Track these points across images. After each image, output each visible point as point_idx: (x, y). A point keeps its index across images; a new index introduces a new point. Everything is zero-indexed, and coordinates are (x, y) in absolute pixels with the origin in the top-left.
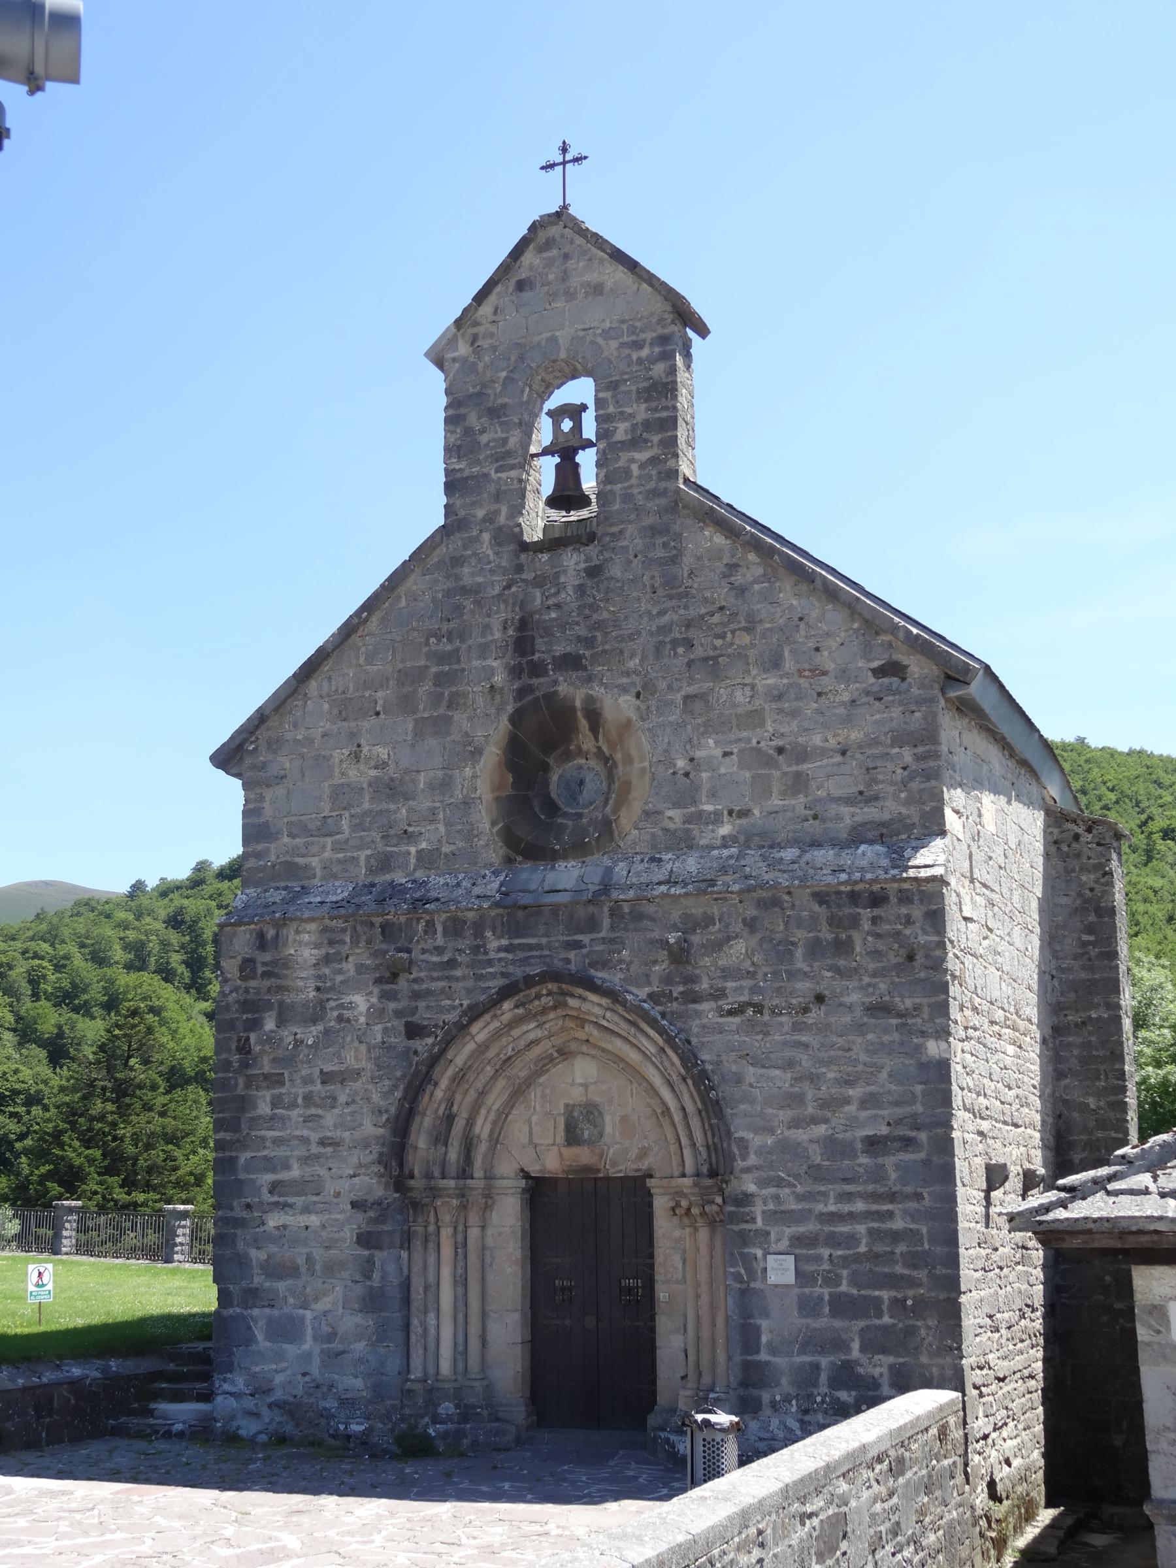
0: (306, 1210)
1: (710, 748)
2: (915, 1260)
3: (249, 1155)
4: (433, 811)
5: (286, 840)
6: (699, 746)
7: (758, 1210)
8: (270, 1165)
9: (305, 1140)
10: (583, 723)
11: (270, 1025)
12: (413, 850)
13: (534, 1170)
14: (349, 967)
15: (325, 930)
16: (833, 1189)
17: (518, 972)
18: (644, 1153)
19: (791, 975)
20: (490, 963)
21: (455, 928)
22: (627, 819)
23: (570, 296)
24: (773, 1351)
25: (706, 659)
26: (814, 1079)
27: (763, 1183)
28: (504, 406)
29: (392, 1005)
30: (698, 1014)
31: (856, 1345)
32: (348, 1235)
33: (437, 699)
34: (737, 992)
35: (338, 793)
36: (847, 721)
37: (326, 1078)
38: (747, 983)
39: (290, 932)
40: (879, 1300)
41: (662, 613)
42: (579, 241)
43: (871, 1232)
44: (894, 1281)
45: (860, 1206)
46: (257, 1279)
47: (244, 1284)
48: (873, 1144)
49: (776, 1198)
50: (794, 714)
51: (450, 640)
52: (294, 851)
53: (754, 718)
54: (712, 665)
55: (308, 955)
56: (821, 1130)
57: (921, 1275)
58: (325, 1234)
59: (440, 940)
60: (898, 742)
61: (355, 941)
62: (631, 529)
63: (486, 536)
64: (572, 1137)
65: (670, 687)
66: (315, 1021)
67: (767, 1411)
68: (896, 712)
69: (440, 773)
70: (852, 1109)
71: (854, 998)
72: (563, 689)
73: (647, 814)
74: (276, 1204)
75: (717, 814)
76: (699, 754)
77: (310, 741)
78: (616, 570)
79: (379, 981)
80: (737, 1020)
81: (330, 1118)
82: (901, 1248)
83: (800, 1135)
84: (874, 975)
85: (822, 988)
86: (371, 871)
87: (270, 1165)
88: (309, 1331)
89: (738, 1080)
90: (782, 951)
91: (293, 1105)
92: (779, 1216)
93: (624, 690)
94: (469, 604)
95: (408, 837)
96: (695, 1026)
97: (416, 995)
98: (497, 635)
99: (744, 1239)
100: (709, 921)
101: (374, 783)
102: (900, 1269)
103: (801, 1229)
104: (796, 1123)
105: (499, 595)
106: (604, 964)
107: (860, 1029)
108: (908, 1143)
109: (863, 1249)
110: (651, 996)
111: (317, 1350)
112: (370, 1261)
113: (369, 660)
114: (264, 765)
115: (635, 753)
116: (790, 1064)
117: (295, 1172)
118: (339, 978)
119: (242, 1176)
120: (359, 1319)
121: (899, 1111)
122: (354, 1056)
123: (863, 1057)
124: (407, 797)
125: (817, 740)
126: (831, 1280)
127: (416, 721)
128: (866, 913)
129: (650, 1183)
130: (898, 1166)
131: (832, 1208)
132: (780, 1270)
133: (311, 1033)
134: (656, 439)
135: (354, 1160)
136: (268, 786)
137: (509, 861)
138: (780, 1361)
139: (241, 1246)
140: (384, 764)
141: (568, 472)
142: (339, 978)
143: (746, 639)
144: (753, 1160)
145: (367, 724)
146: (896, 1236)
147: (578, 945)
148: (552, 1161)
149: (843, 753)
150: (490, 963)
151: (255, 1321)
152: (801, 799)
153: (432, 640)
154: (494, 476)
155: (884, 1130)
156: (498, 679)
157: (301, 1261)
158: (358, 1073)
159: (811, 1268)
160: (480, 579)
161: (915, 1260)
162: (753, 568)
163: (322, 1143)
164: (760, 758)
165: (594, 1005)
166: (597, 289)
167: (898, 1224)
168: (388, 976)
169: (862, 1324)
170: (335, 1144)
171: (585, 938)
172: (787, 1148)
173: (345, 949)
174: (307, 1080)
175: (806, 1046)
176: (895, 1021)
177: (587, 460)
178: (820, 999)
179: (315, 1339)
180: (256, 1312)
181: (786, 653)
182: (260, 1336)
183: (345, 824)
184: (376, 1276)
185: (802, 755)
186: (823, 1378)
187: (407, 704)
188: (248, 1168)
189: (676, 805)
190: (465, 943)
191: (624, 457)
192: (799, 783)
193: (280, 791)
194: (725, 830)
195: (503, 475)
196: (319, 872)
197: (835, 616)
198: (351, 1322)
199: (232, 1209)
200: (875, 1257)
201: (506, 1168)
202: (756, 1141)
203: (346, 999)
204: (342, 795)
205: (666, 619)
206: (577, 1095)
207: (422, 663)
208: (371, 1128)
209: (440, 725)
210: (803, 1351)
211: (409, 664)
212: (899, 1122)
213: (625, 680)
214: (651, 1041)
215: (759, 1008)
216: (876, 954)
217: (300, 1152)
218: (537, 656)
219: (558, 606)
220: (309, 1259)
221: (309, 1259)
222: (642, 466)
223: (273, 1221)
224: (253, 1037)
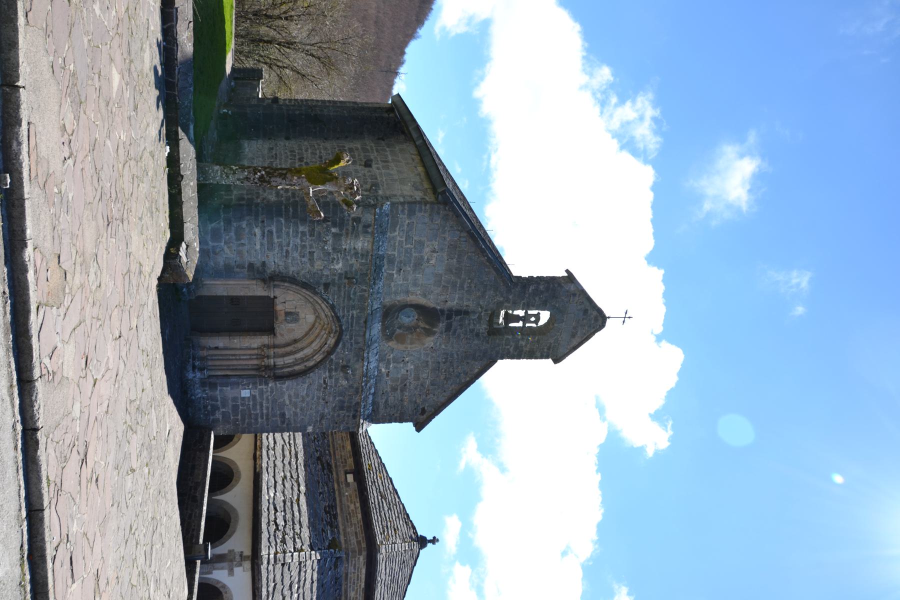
0: (262, 244)
1: (411, 367)
2: (250, 424)
3: (283, 222)
7: (264, 387)
8: (279, 231)
9: (288, 245)
10: (427, 327)
11: (333, 230)
13: (277, 301)
14: (353, 261)
15: (368, 252)
16: (270, 405)
17: (344, 321)
18: (282, 335)
20: (348, 311)
21: (363, 299)
22: (392, 344)
23: (574, 328)
26: (303, 401)
27: (271, 388)
29: (337, 278)
32: (253, 260)
35: (421, 244)
37: (312, 253)
39: (369, 238)
42: (593, 330)
44: (243, 420)
45: (265, 411)
46: (235, 224)
48: (283, 415)
50: (416, 389)
53: (417, 378)
55: (359, 245)
56: (287, 402)
57: (245, 425)
58: (253, 251)
59: (358, 294)
61: (362, 264)
63: (502, 299)
64: (287, 314)
66: (334, 249)
71: (326, 411)
72: (441, 325)
73: (393, 350)
74: (264, 233)
77: (444, 233)
79: (346, 272)
81: (296, 255)
83: (286, 397)
87: (279, 231)
88: (216, 244)
91: (302, 241)
92: (261, 393)
93: (435, 344)
96: (321, 372)
97: (339, 287)
99: (254, 384)
100: (354, 375)
102: (247, 421)
104: (290, 396)
105: (479, 304)
106: (344, 346)
108: (283, 422)
111: (210, 247)
112: (243, 267)
114: (438, 213)
116: (307, 395)
117: (276, 240)
118: (349, 258)
120: (222, 263)
121: (292, 421)
122: (318, 265)
124: (414, 271)
126: (243, 405)
127: (441, 275)
132: (245, 393)
133: (329, 248)
135: (280, 263)
137: (384, 307)
138: (218, 392)
139: (248, 218)
141: (517, 318)
142: (349, 258)
144: (278, 385)
146: (256, 419)
147: (351, 339)
148: (279, 307)
150: (348, 311)
151: (219, 223)
156: (449, 303)
157: (242, 241)
158: (313, 266)
161: (250, 424)
163: (287, 251)
165: (331, 341)
166: (573, 336)
167: (260, 420)
168: (348, 277)
170: (287, 257)
172: (283, 394)
173: (360, 260)
174: (311, 246)
177: (520, 324)
179: (213, 246)
180: (222, 223)
182: (213, 225)
183: (409, 246)
184: (238, 270)
188: (278, 221)
189: (394, 358)
190: (356, 302)
191: (513, 344)
193: (427, 220)
194: (383, 370)
197: (443, 399)
198: (221, 261)
200: (250, 415)
201: (277, 292)
202: (285, 386)
203: (341, 261)
205: (455, 356)
206: (302, 315)
208: (292, 269)
214: (318, 358)
215: (325, 388)
216: (339, 416)
217: (284, 243)
219: (469, 324)
220: (243, 245)
221: (243, 245)
223: (257, 231)
224: (329, 223)
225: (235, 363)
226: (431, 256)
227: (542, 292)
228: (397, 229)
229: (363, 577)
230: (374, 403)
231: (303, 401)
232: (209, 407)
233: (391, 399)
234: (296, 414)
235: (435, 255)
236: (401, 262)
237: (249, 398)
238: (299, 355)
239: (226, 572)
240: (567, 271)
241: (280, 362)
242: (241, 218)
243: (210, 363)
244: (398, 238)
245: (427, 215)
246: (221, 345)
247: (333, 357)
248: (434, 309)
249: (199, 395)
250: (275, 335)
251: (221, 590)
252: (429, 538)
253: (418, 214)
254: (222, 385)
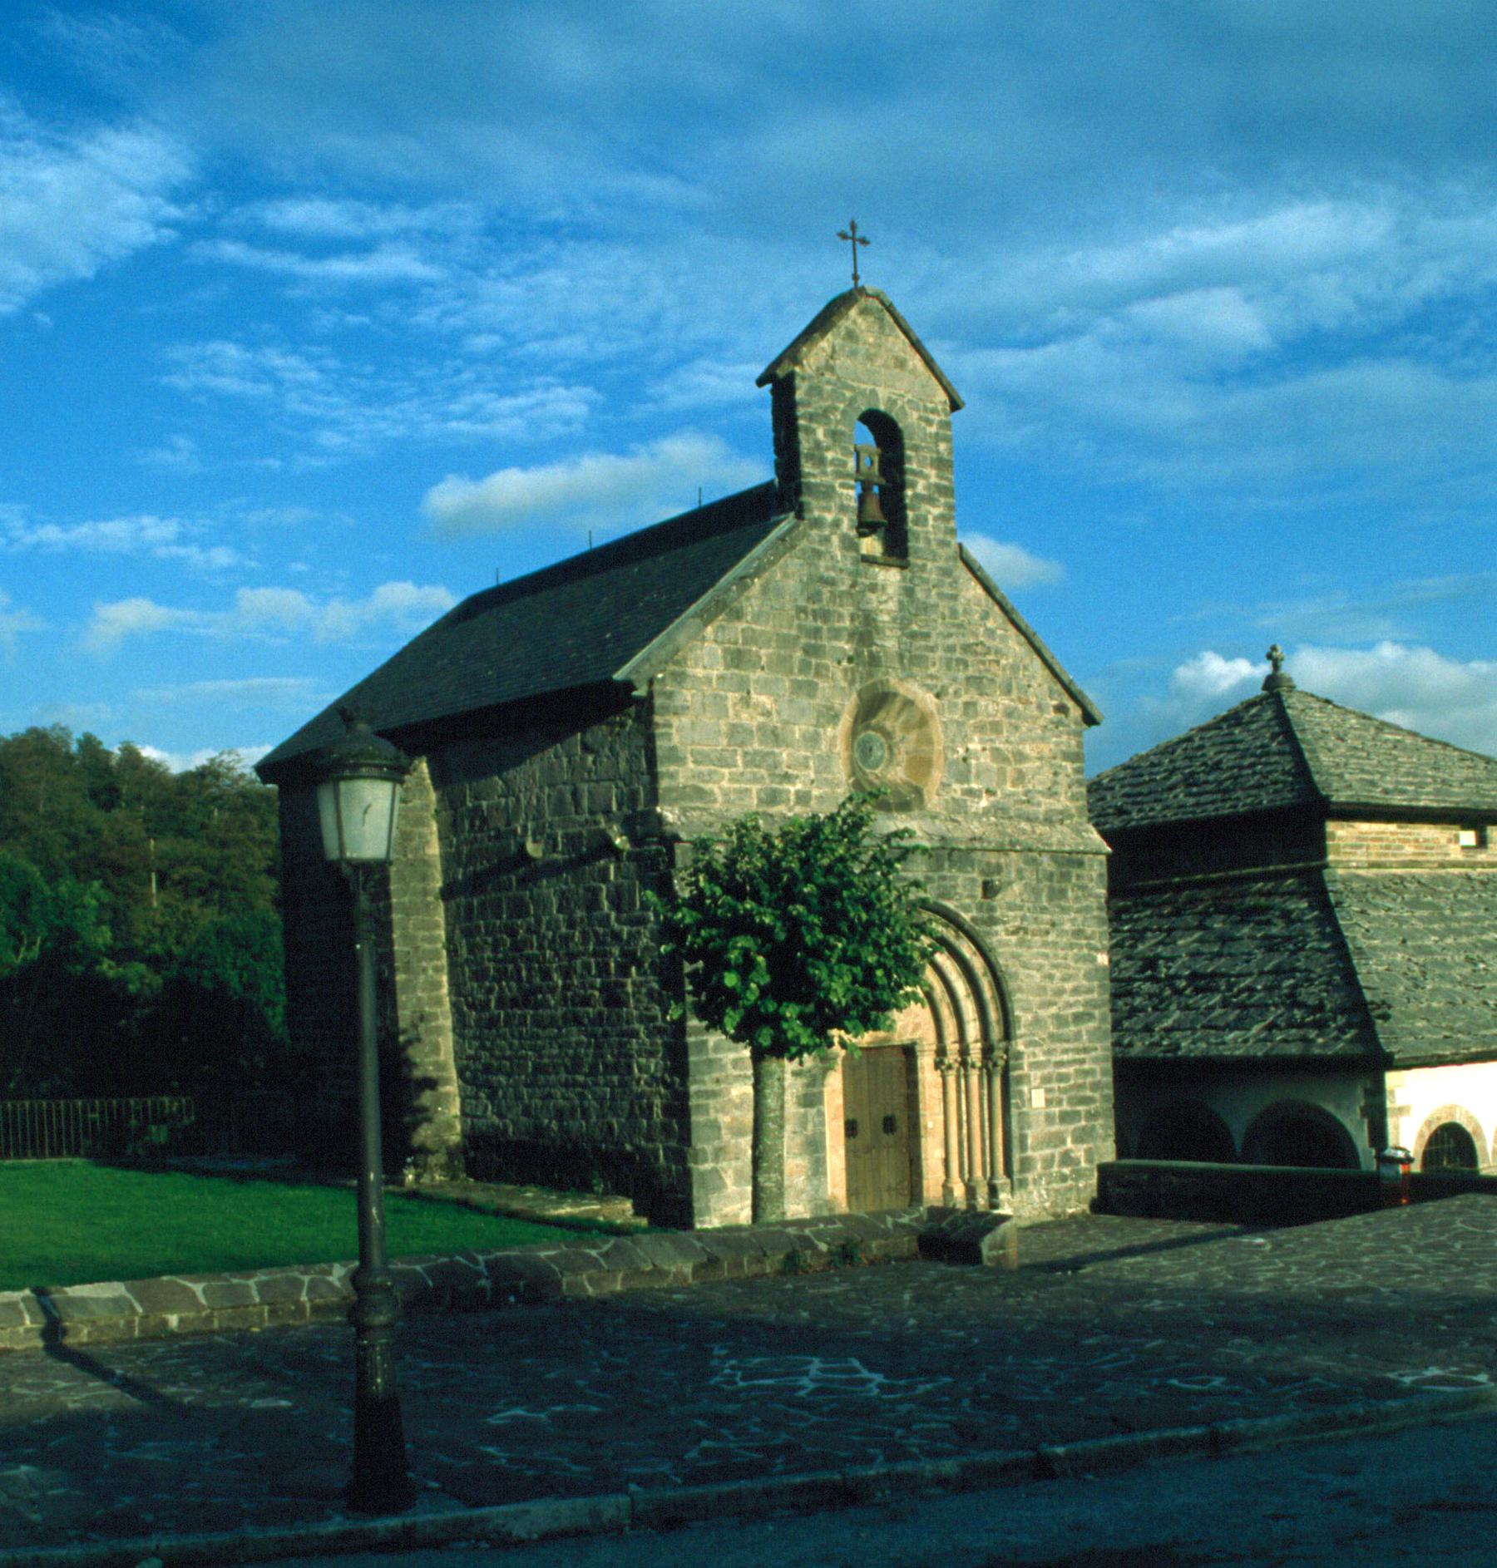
4: (806, 758)
5: (691, 765)
6: (971, 740)
7: (1026, 1062)
12: (792, 789)
16: (1059, 1046)
18: (917, 1026)
19: (1043, 910)
24: (1033, 1149)
25: (975, 678)
26: (1051, 977)
28: (843, 433)
30: (996, 933)
31: (1069, 1140)
33: (805, 667)
34: (1013, 919)
36: (1043, 739)
38: (1019, 913)
40: (1078, 1113)
41: (950, 635)
43: (1077, 1071)
47: (716, 1143)
48: (1078, 1018)
49: (1034, 1055)
51: (815, 619)
52: (700, 776)
53: (996, 727)
54: (975, 682)
56: (1053, 1010)
57: (1097, 1095)
60: (1067, 756)
62: (930, 565)
63: (835, 539)
65: (956, 693)
67: (1031, 1187)
68: (1064, 738)
69: (812, 729)
70: (1066, 997)
71: (1068, 927)
75: (980, 791)
76: (971, 746)
77: (708, 680)
78: (920, 594)
80: (1014, 939)
82: (1089, 1080)
83: (1043, 1013)
84: (1079, 911)
85: (1055, 918)
86: (761, 801)
89: (1015, 976)
90: (1036, 892)
92: (1036, 1065)
93: (930, 688)
94: (826, 591)
95: (787, 778)
98: (847, 623)
99: (1020, 1080)
101: (761, 727)
102: (1088, 1093)
103: (1046, 1071)
106: (943, 896)
107: (1072, 946)
108: (1091, 1017)
109: (1072, 1082)
110: (973, 919)
112: (805, 1115)
113: (757, 618)
115: (935, 738)
116: (1039, 968)
119: (712, 1056)
121: (1089, 997)
123: (1072, 964)
125: (1027, 749)
126: (1060, 1102)
127: (794, 682)
128: (1074, 872)
129: (918, 1048)
130: (1088, 1032)
131: (1058, 1059)
132: (1038, 1098)
134: (942, 500)
136: (676, 714)
139: (712, 1115)
140: (768, 714)
143: (994, 668)
145: (755, 675)
146: (1087, 1073)
149: (1040, 758)
152: (1020, 789)
153: (802, 615)
154: (839, 490)
155: (1081, 1009)
159: (1050, 1096)
160: (833, 574)
162: (996, 620)
164: (997, 754)
167: (1086, 1067)
169: (1071, 1127)
171: (935, 876)
172: (1037, 1021)
175: (1046, 956)
176: (1084, 942)
178: (1053, 925)
180: (724, 1164)
181: (1014, 685)
182: (729, 1181)
184: (810, 1127)
185: (1021, 757)
186: (1057, 1159)
187: (781, 664)
191: (925, 507)
192: (1020, 778)
193: (685, 720)
194: (984, 802)
195: (845, 491)
196: (720, 799)
199: (703, 1082)
204: (737, 733)
205: (951, 641)
207: (794, 632)
209: (810, 689)
210: (1048, 1146)
211: (785, 631)
212: (1087, 1004)
213: (929, 682)
214: (967, 949)
218: (874, 648)
222: (936, 519)
225: (976, 1123)
226: (757, 705)
227: (818, 445)
228: (708, 787)
230: (1048, 820)
231: (1051, 977)
232: (1066, 1171)
234: (1076, 991)
235: (754, 696)
236: (772, 775)
237: (1048, 1091)
238: (961, 987)
240: (761, 382)
241: (973, 1030)
242: (715, 1126)
243: (978, 1173)
244: (725, 784)
245: (675, 721)
246: (939, 1153)
247: (966, 917)
248: (859, 695)
249: (1043, 1192)
250: (914, 1044)
251: (1434, 1127)
253: (676, 740)
254: (1023, 1147)
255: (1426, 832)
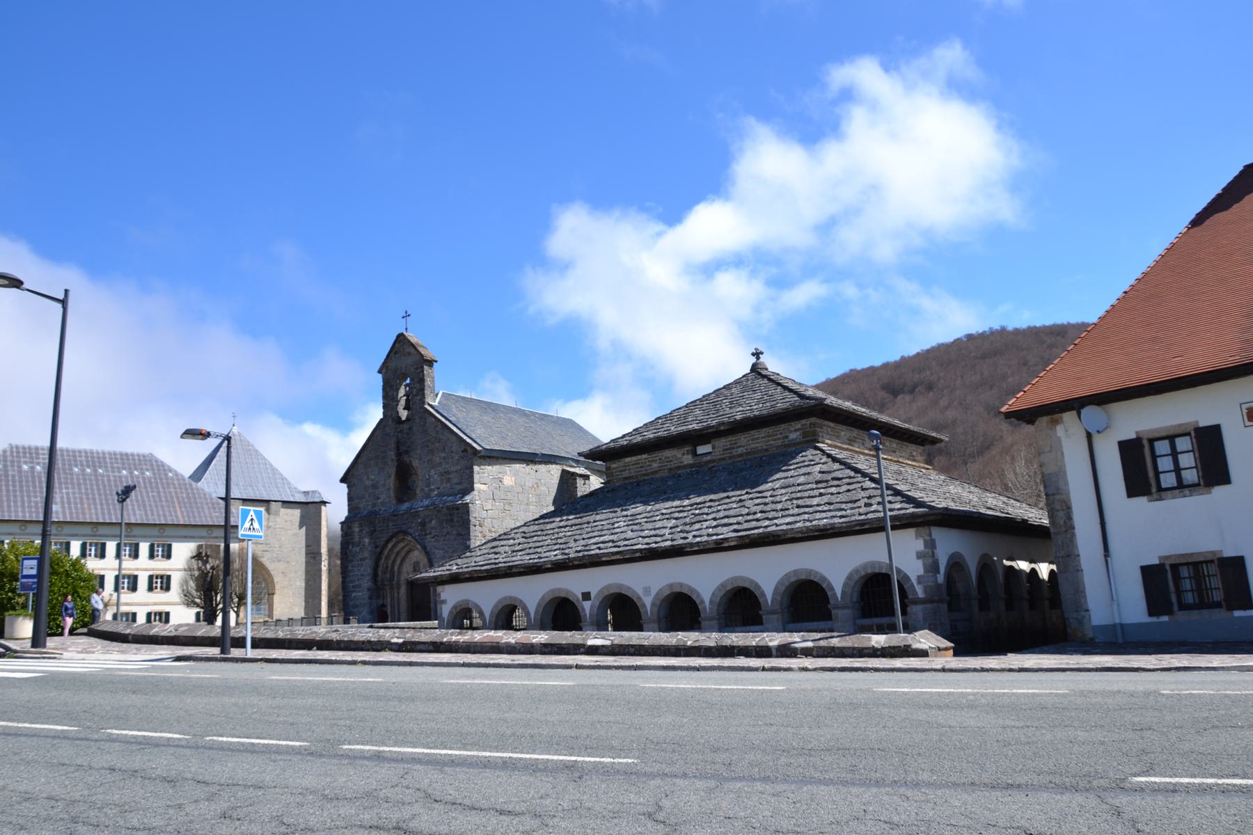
1: (432, 472)
55: (357, 530)
122: (366, 554)
133: (357, 549)
164: (441, 474)
166: (409, 354)
168: (371, 533)
192: (449, 480)
208: (370, 571)
229: (634, 458)
233: (455, 481)
239: (444, 606)
252: (754, 360)
255: (668, 453)
